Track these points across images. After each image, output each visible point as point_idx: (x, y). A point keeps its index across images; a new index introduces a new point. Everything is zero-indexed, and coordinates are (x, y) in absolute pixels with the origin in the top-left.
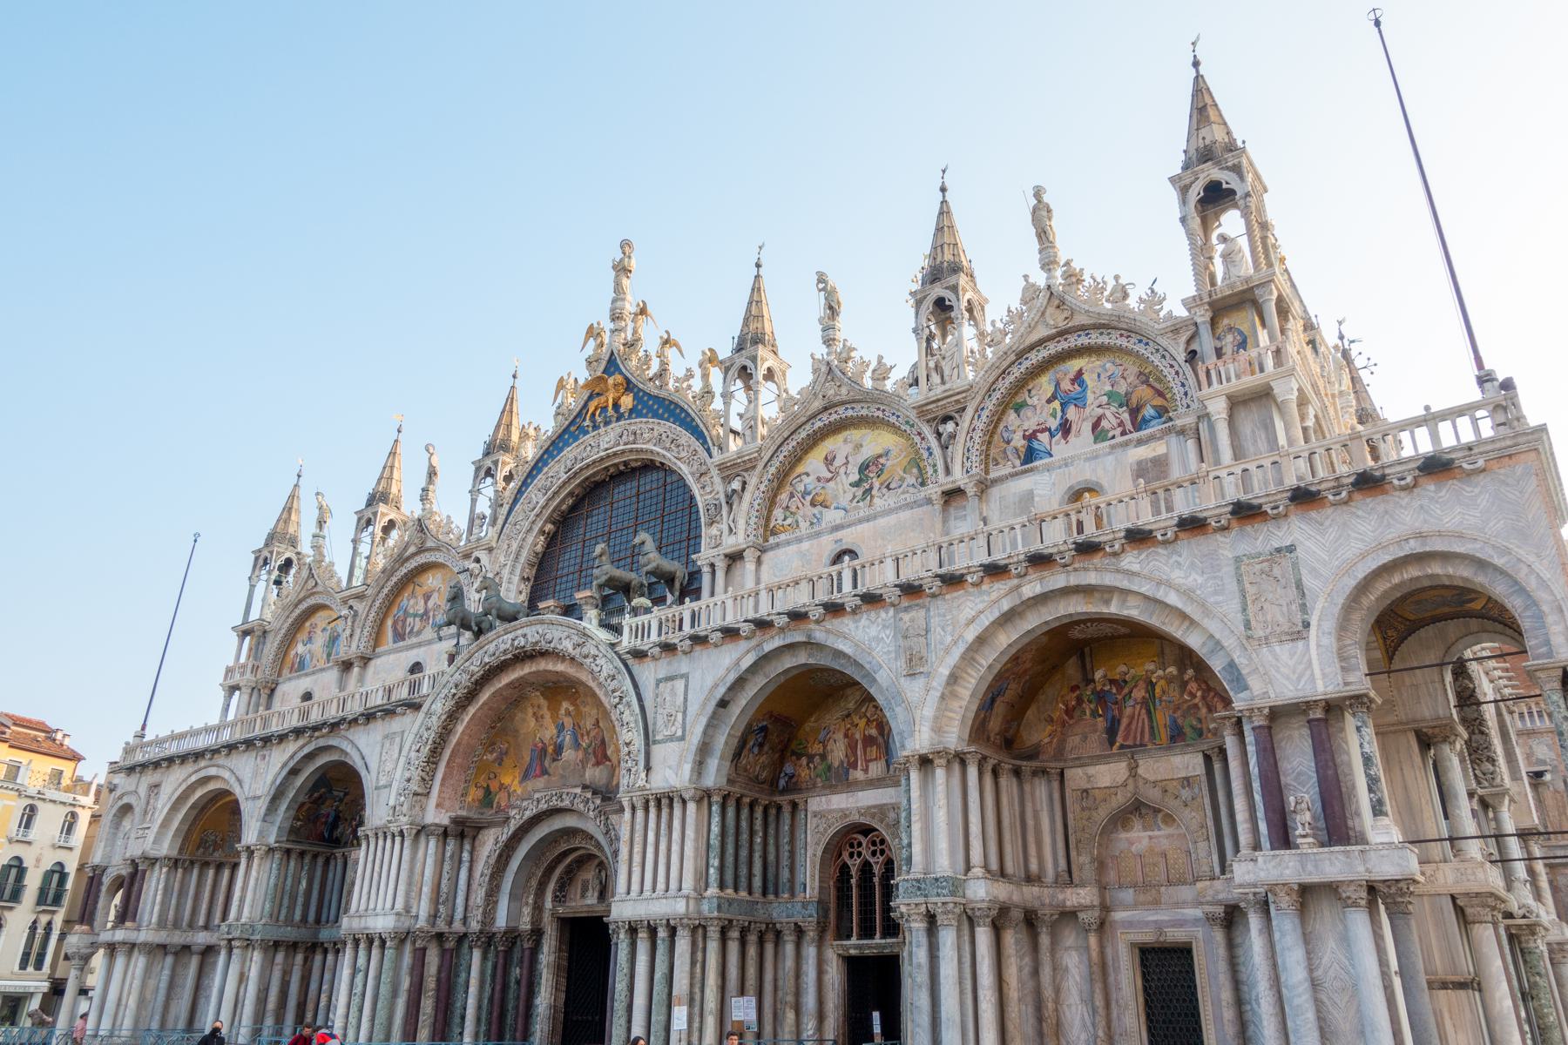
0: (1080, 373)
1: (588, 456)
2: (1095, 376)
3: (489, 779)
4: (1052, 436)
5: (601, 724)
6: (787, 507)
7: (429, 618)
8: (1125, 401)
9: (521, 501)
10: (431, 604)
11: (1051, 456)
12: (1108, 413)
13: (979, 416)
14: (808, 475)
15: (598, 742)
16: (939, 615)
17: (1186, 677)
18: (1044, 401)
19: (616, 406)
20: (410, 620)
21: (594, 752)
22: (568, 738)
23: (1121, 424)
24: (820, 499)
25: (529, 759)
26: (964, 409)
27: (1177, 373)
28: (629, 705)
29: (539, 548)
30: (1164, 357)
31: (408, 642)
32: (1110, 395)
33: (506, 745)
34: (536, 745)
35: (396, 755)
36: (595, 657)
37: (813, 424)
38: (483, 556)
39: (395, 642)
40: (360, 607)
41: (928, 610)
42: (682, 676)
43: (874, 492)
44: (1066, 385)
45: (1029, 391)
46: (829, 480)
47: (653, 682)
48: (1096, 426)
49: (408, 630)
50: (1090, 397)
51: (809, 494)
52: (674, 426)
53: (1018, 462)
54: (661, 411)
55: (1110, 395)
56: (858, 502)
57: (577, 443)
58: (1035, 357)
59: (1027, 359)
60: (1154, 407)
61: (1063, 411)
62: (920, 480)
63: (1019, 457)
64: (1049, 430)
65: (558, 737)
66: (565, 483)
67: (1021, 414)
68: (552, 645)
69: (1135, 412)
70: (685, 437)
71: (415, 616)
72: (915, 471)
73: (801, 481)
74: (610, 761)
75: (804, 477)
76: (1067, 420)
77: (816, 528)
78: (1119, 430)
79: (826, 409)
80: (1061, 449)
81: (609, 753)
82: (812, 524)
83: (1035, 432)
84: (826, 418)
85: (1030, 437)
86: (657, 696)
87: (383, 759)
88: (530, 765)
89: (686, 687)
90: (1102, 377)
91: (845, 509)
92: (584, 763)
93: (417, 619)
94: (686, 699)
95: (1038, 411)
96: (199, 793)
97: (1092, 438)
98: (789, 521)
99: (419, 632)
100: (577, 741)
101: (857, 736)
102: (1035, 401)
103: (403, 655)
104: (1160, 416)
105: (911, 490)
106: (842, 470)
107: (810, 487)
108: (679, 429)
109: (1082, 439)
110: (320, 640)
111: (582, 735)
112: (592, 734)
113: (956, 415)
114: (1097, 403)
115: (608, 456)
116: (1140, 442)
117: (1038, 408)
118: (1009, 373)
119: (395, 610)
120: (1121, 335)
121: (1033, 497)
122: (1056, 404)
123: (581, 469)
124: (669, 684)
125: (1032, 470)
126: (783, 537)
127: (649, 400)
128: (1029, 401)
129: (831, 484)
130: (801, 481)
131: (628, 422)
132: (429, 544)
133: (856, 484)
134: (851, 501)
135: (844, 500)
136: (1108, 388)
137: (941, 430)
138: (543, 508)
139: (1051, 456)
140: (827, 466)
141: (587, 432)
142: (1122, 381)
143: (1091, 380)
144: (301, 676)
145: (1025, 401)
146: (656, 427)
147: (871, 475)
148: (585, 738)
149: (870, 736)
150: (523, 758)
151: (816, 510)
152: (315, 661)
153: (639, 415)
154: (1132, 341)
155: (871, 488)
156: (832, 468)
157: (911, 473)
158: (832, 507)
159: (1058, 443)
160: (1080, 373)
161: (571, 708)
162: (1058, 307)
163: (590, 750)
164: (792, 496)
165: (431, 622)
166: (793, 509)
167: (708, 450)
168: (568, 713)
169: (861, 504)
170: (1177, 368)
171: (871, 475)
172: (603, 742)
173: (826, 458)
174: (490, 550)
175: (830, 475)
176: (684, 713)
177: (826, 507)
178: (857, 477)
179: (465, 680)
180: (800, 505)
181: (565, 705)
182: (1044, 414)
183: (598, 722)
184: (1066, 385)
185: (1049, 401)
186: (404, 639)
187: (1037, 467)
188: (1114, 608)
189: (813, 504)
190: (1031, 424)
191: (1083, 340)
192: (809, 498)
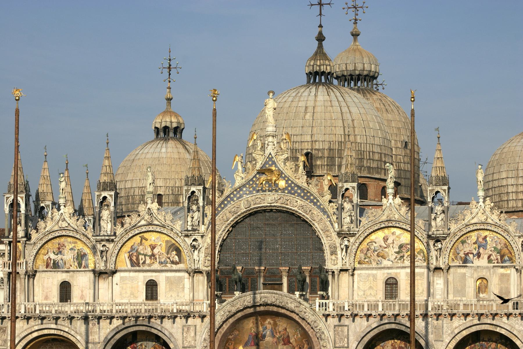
0: (486, 237)
1: (259, 204)
2: (491, 240)
3: (229, 345)
4: (474, 256)
5: (287, 330)
6: (366, 254)
7: (156, 259)
8: (499, 252)
9: (219, 215)
10: (156, 251)
11: (473, 263)
12: (493, 254)
13: (450, 243)
14: (376, 243)
15: (285, 336)
16: (447, 324)
17: (507, 344)
18: (472, 243)
19: (276, 185)
20: (140, 257)
21: (283, 340)
22: (268, 333)
23: (497, 259)
24: (381, 254)
25: (248, 338)
26: (445, 239)
27: (517, 250)
28: (323, 333)
29: (225, 237)
30: (514, 243)
31: (141, 268)
32: (495, 248)
33: (238, 332)
34: (252, 334)
35: (193, 334)
36: (305, 313)
37: (381, 224)
38: (199, 238)
39: (132, 266)
40: (111, 246)
41: (443, 321)
42: (346, 326)
43: (405, 258)
44: (480, 240)
45: (468, 237)
46: (386, 248)
47: (333, 327)
48: (489, 257)
49: (141, 262)
50: (488, 247)
51: (376, 251)
52: (310, 204)
53: (461, 262)
54: (302, 194)
55: (495, 248)
56: (398, 260)
57: (252, 195)
58: (472, 228)
59: (469, 227)
60: (508, 257)
61: (478, 248)
62: (424, 258)
63: (462, 261)
64: (473, 254)
65: (263, 331)
66: (245, 212)
67: (464, 245)
68: (283, 304)
69: (502, 256)
70: (316, 211)
71: (145, 255)
72: (422, 254)
73: (372, 244)
74: (292, 344)
75: (374, 243)
76: (479, 252)
77: (379, 266)
78: (496, 261)
79: (387, 221)
80: (477, 263)
81: (291, 341)
82: (377, 264)
83: (468, 253)
84: (387, 224)
85: (467, 254)
86: (335, 331)
87: (185, 335)
88: (248, 341)
89: (348, 330)
90: (493, 241)
91: (392, 261)
92: (277, 343)
93: (147, 258)
94: (348, 335)
95: (470, 246)
96: (35, 335)
97: (487, 261)
98: (367, 260)
99: (150, 265)
100: (273, 334)
101: (397, 346)
102: (469, 241)
103: (141, 275)
104: (510, 261)
105: (420, 261)
106: (391, 245)
107: (377, 249)
108: (313, 206)
109: (483, 262)
110: (68, 256)
111: (276, 333)
112: (282, 333)
113: (442, 241)
114: (490, 249)
115: (271, 206)
116: (502, 267)
117: (470, 244)
118: (462, 231)
119: (127, 248)
120: (502, 231)
121: (466, 276)
122: (476, 246)
123: (254, 208)
124: (340, 328)
125: (466, 266)
126: (364, 266)
127: (295, 186)
128: (467, 241)
129: (387, 250)
130: (372, 244)
131: (283, 194)
132: (156, 222)
133: (397, 253)
134: (395, 259)
135: (392, 258)
136: (494, 245)
137: (436, 245)
138: (232, 221)
139: (473, 263)
140: (384, 241)
141: (258, 191)
142: (499, 244)
143: (489, 241)
144: (59, 271)
145: (466, 240)
146: (299, 201)
147: (404, 251)
148: (278, 334)
149: (402, 347)
150: (244, 338)
151: (380, 259)
152: (68, 265)
153: (290, 192)
154: (505, 234)
155: (403, 256)
156: (387, 244)
157: (420, 255)
158: (387, 259)
159: (476, 260)
160: (486, 237)
161: (272, 322)
162: (483, 214)
163: (281, 339)
164: (368, 250)
165: (158, 260)
166: (369, 255)
167: (330, 221)
168: (270, 323)
169: (399, 261)
170: (518, 248)
171: (404, 251)
172: (288, 336)
173: (384, 238)
174: (202, 236)
175: (386, 246)
176: (348, 339)
177: (385, 259)
178: (397, 250)
179: (234, 310)
180: (372, 255)
181: (269, 320)
182: (472, 247)
183: (286, 329)
184: (480, 240)
185: (474, 243)
186: (140, 266)
187: (468, 266)
188: (498, 330)
189: (378, 255)
190: (467, 250)
191: (489, 228)
192: (376, 253)
